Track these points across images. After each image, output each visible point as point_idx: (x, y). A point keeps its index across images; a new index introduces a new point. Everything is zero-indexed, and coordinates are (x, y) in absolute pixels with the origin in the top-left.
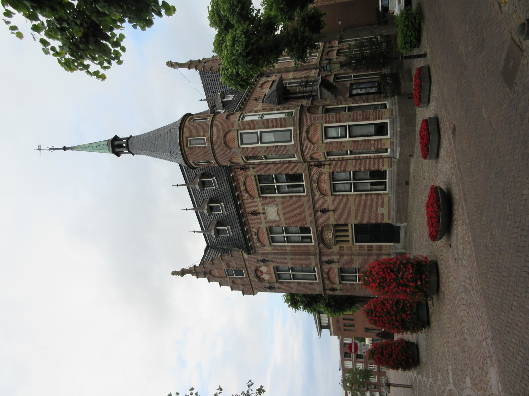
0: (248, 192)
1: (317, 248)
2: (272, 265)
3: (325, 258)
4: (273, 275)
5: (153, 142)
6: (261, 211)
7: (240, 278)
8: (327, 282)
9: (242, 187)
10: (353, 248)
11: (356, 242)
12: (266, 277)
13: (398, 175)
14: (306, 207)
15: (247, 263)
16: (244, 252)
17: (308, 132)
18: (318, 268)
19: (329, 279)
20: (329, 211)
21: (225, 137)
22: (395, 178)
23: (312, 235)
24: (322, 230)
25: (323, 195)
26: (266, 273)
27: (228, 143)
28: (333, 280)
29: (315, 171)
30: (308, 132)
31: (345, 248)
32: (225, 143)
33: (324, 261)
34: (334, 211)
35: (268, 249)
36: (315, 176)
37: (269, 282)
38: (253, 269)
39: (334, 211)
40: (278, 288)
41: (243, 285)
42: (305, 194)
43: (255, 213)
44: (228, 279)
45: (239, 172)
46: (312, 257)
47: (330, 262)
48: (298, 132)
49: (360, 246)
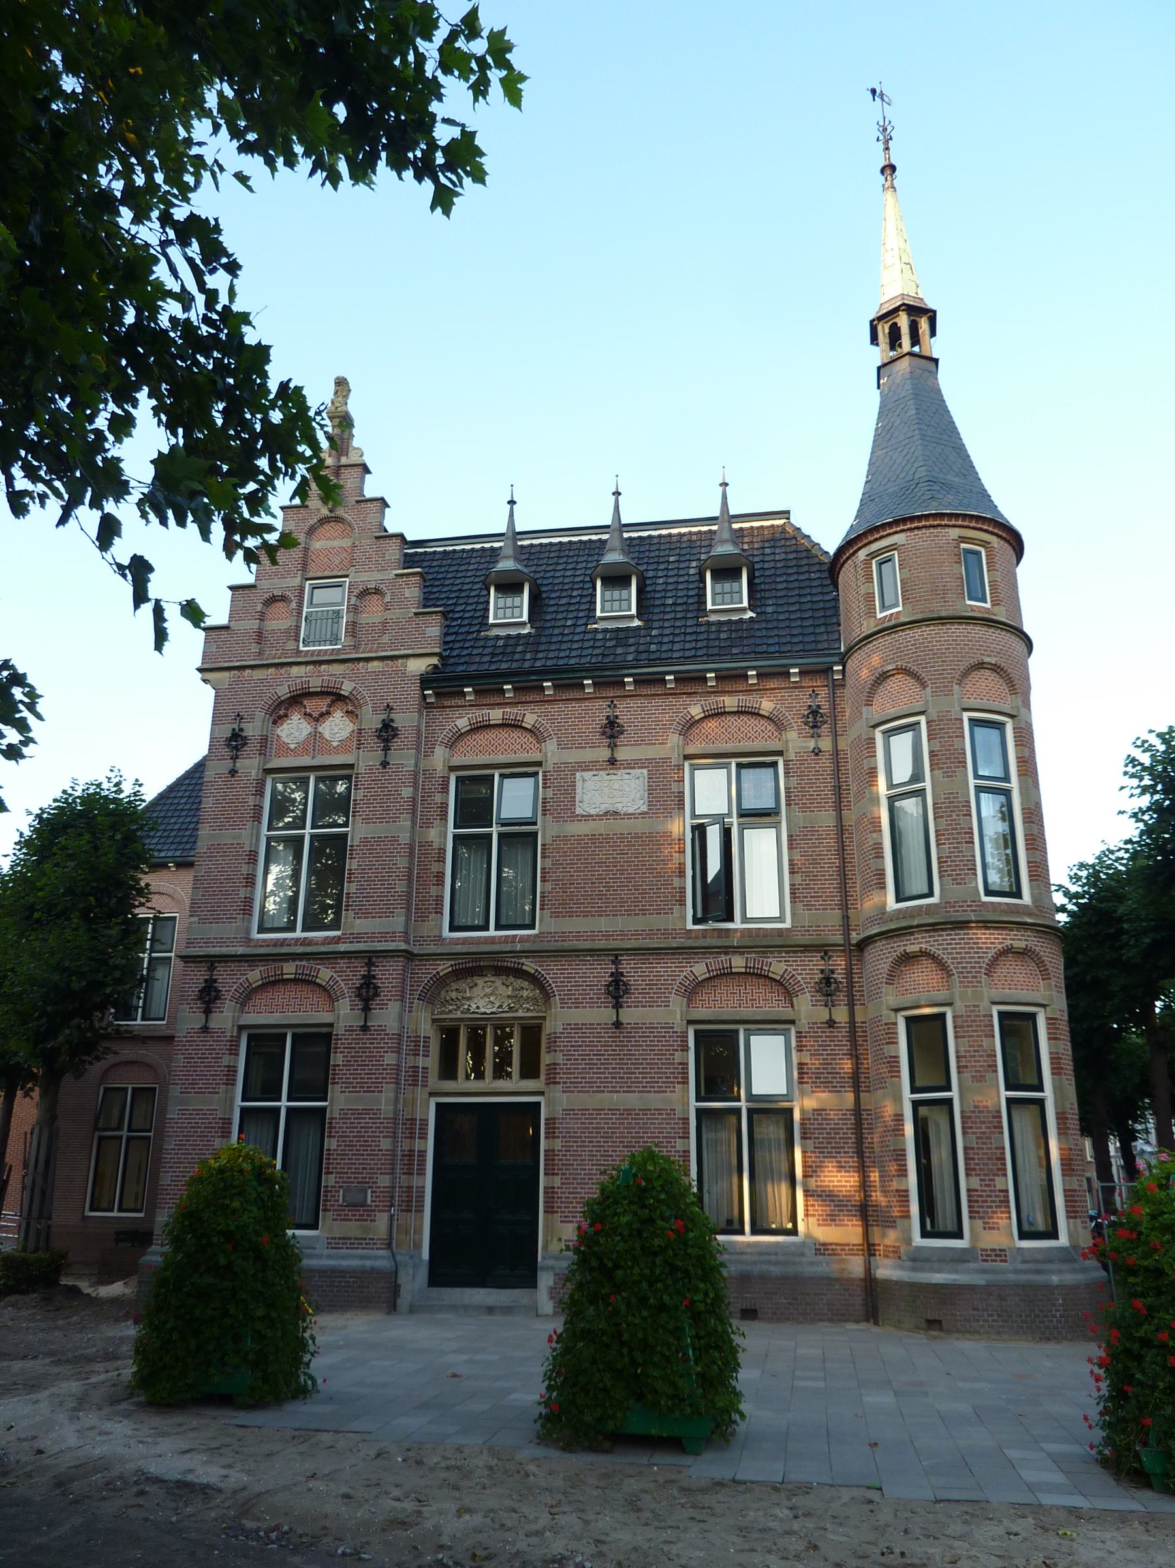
1: (432, 949)
2: (367, 760)
3: (388, 974)
4: (306, 761)
5: (945, 437)
6: (622, 754)
7: (298, 627)
8: (255, 975)
9: (730, 702)
10: (420, 1093)
11: (438, 1105)
12: (294, 729)
13: (784, 1279)
14: (637, 923)
15: (375, 665)
16: (435, 661)
17: (1024, 953)
18: (337, 940)
19: (269, 984)
20: (617, 1006)
21: (996, 668)
22: (775, 1270)
23: (492, 932)
24: (519, 973)
25: (693, 990)
26: (316, 736)
27: (976, 675)
28: (259, 1000)
29: (807, 970)
30: (1024, 954)
31: (421, 1062)
32: (980, 666)
33: (376, 971)
34: (618, 1025)
35: (439, 758)
36: (777, 967)
37: (264, 741)
38: (347, 688)
39: (618, 1025)
40: (233, 772)
41: (260, 636)
42: (690, 926)
43: (612, 730)
44: (297, 581)
45: (801, 701)
46: (397, 922)
47: (367, 993)
48: (1029, 920)
49: (424, 1122)
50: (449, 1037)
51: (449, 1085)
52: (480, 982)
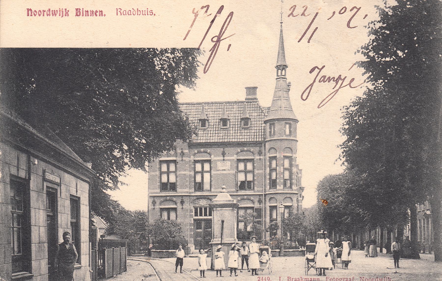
0: (241, 151)
3: (185, 199)
43: (224, 154)
47: (182, 202)
50: (196, 209)
51: (196, 218)
52: (201, 200)
